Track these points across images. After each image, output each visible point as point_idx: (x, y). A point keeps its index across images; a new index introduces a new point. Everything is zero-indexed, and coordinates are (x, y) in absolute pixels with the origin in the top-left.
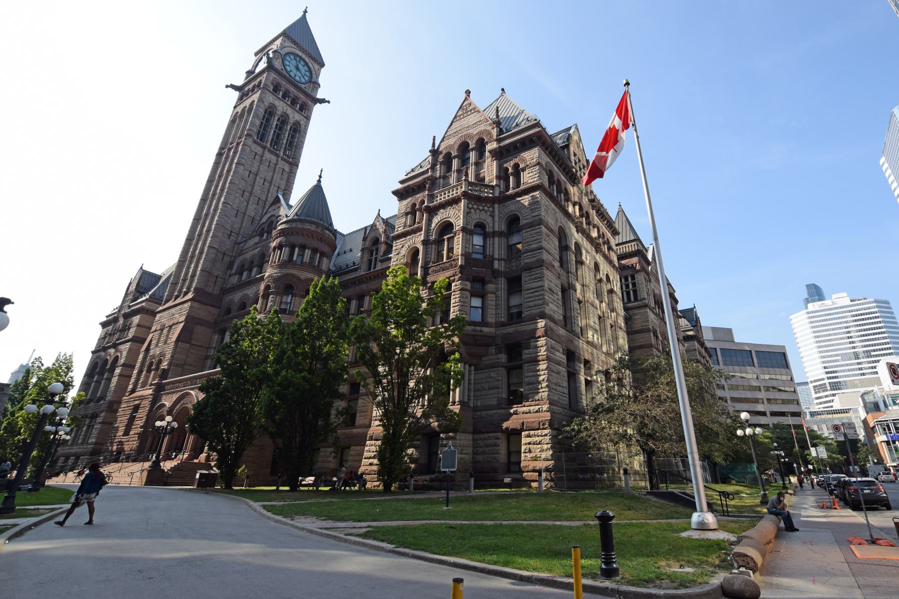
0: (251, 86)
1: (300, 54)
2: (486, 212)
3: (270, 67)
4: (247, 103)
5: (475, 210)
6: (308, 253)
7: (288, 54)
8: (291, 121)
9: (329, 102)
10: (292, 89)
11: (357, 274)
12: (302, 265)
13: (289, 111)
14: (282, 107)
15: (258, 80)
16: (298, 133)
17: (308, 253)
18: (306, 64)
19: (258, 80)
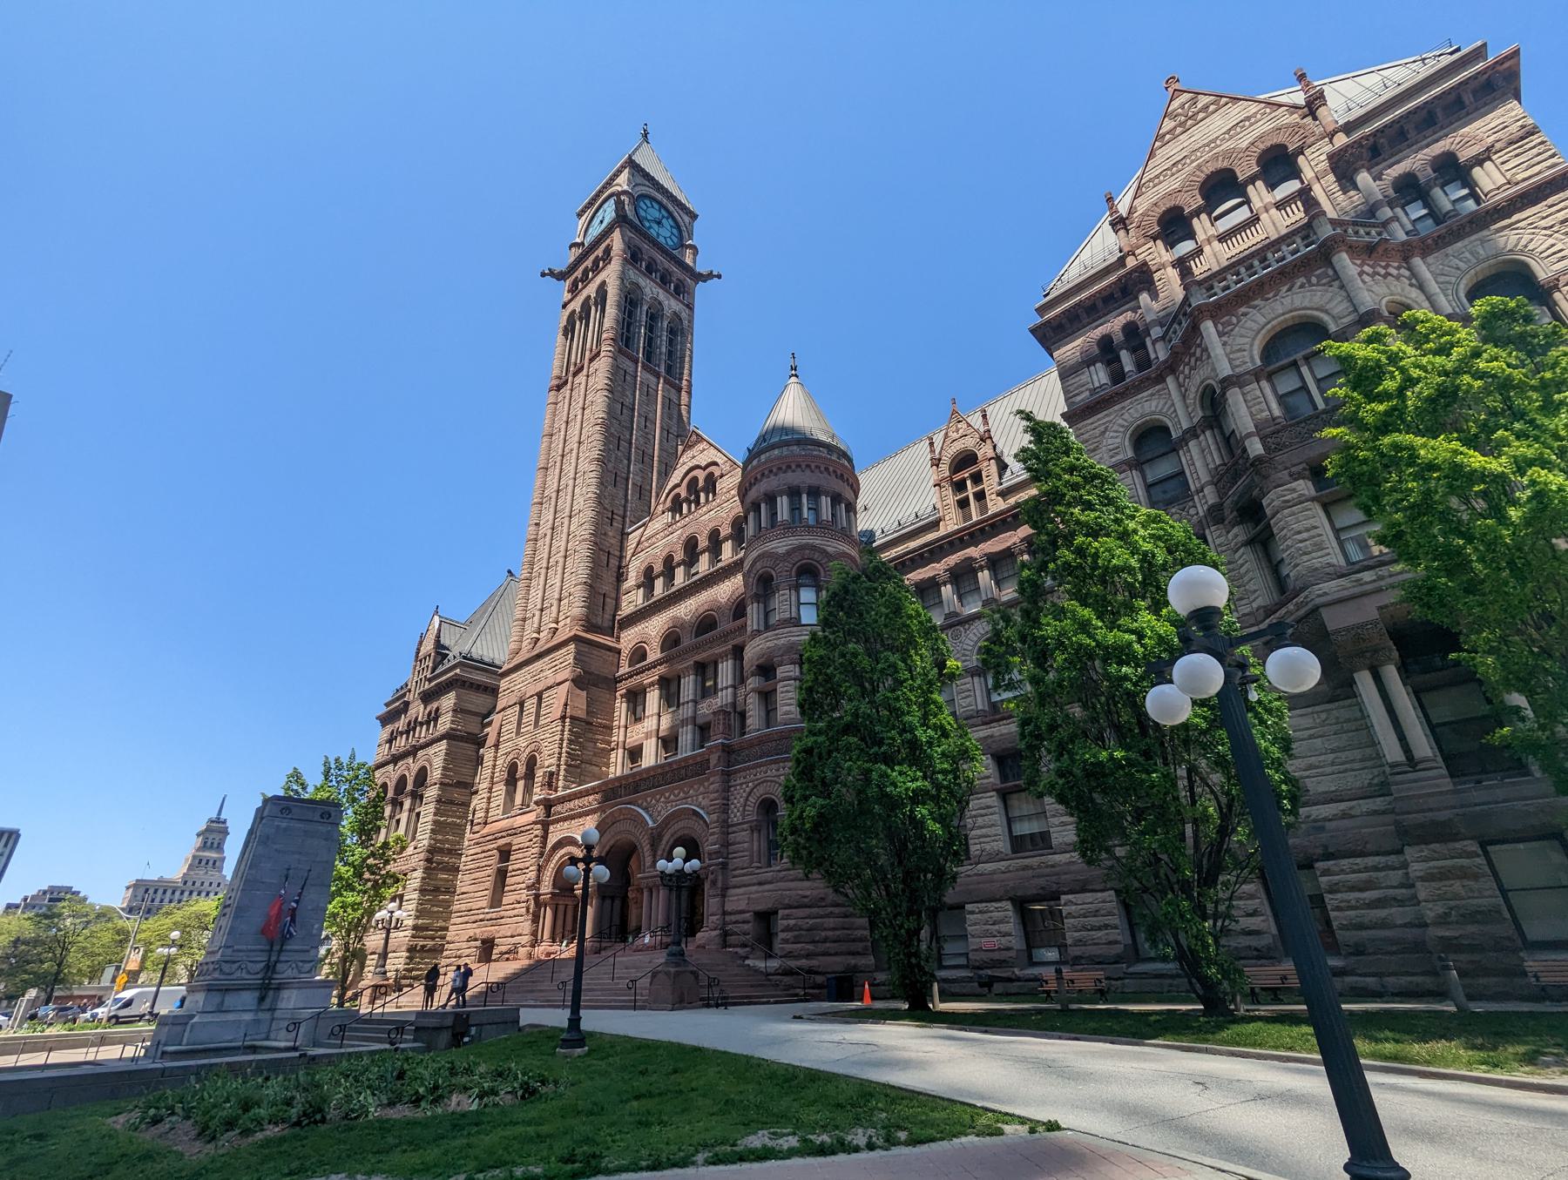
0: (589, 263)
1: (659, 196)
2: (1398, 278)
3: (621, 220)
4: (591, 290)
5: (1372, 276)
6: (825, 502)
7: (643, 196)
8: (668, 312)
9: (719, 276)
10: (659, 257)
11: (943, 530)
12: (820, 526)
13: (662, 296)
14: (650, 289)
15: (603, 246)
16: (679, 331)
17: (825, 502)
18: (671, 215)
19: (603, 246)
